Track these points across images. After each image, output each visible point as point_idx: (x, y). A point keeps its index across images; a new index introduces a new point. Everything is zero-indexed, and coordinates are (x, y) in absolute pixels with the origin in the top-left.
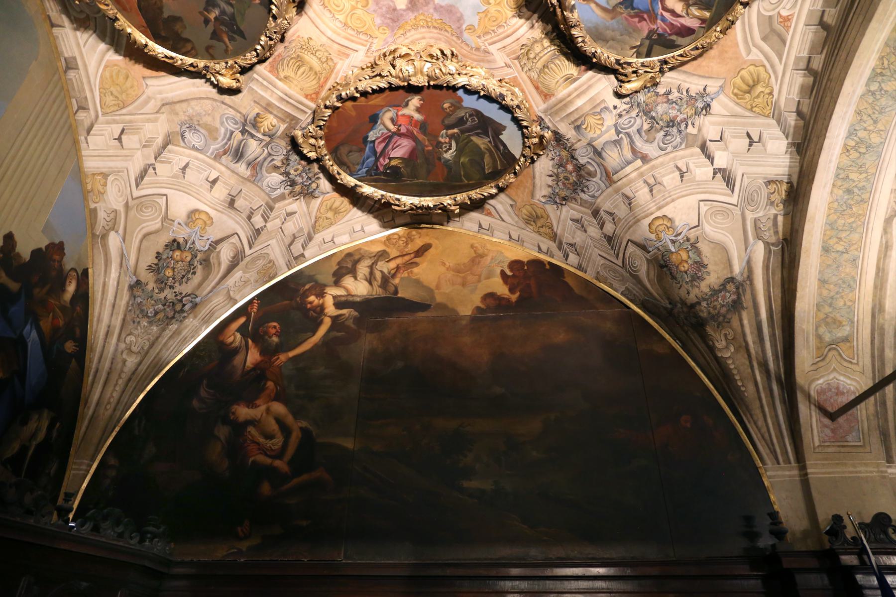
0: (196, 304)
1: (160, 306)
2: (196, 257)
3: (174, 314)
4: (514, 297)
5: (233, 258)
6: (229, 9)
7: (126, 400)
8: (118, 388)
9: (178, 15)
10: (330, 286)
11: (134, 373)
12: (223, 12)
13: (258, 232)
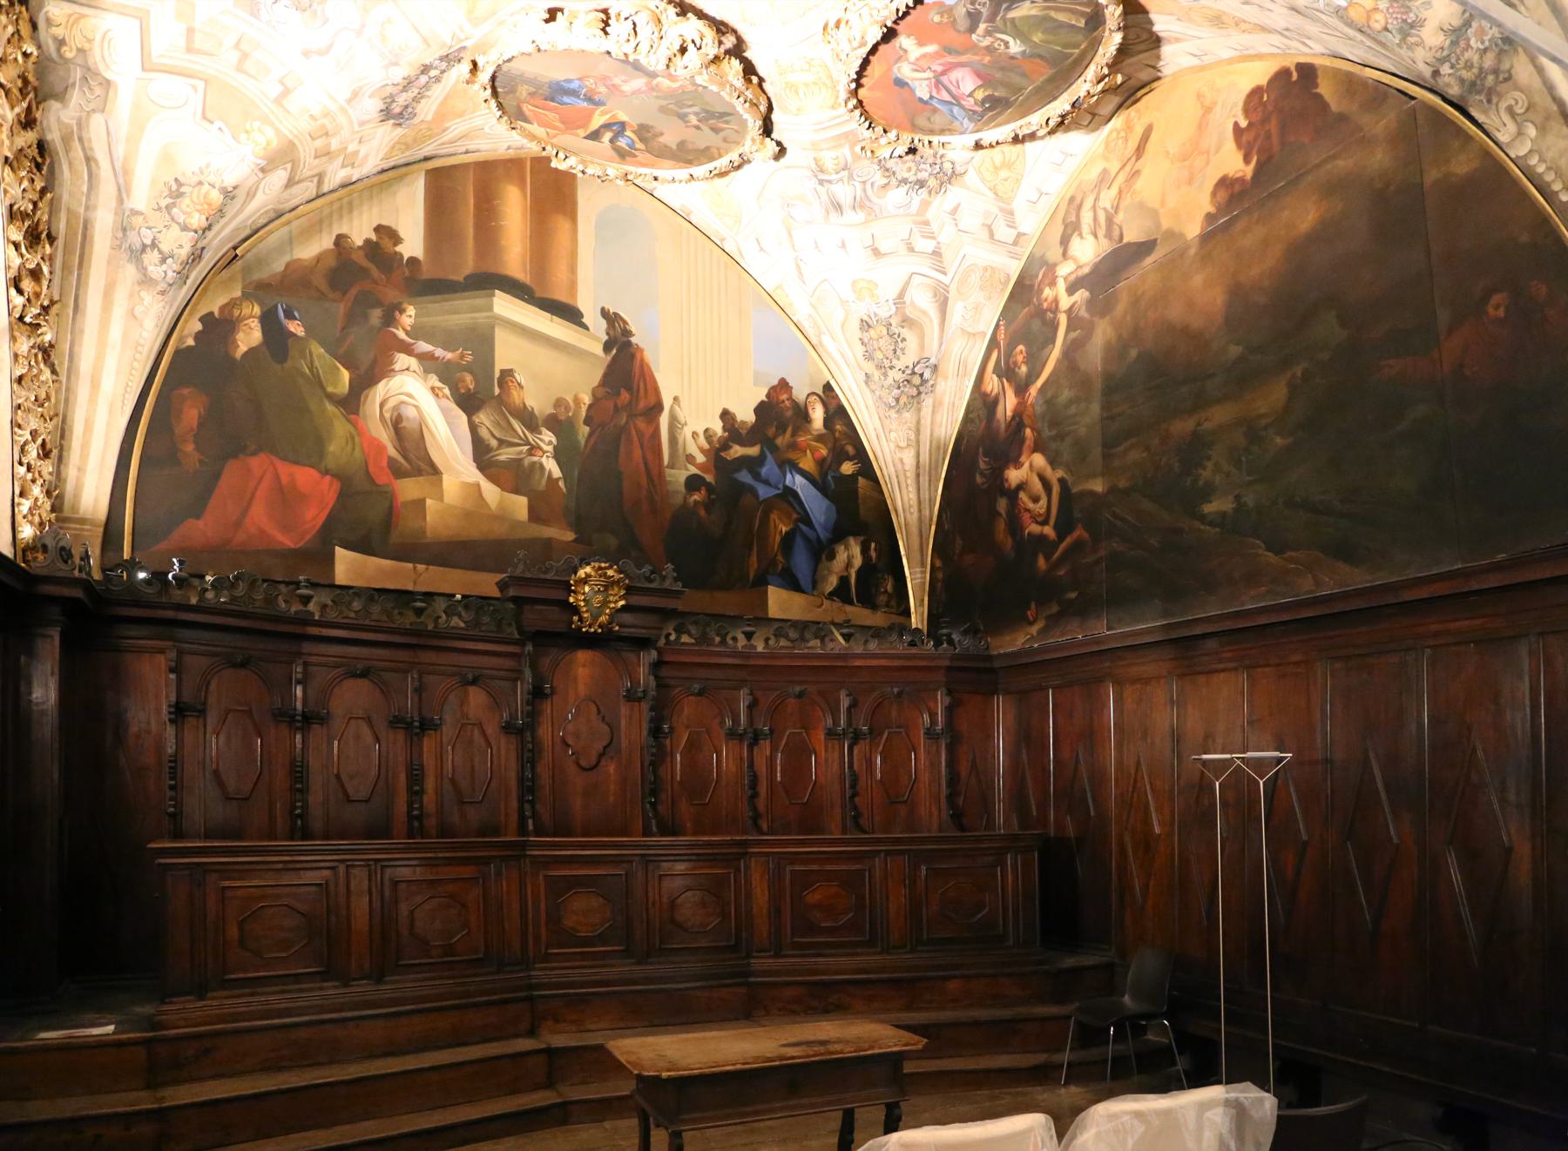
0: (935, 366)
1: (896, 392)
2: (891, 325)
3: (918, 389)
4: (1248, 171)
5: (935, 296)
6: (695, 109)
7: (927, 496)
8: (910, 489)
9: (679, 140)
10: (1061, 262)
11: (918, 467)
12: (696, 114)
13: (936, 253)
